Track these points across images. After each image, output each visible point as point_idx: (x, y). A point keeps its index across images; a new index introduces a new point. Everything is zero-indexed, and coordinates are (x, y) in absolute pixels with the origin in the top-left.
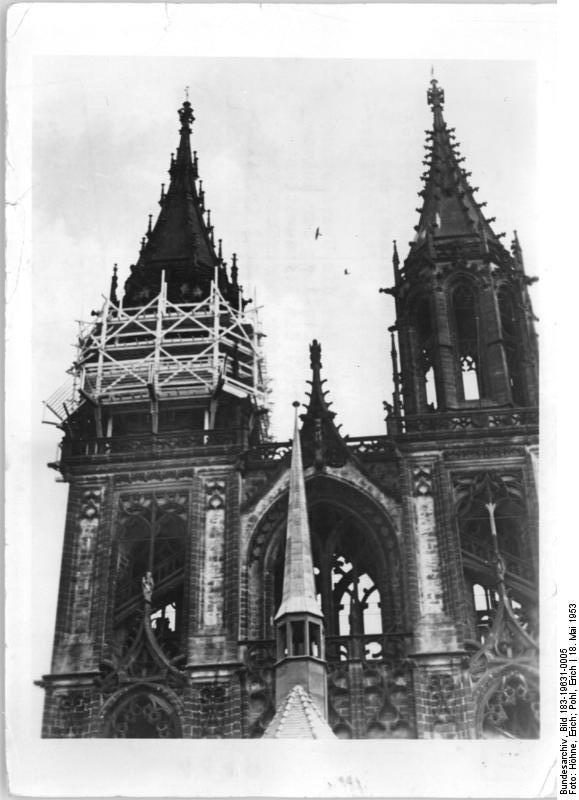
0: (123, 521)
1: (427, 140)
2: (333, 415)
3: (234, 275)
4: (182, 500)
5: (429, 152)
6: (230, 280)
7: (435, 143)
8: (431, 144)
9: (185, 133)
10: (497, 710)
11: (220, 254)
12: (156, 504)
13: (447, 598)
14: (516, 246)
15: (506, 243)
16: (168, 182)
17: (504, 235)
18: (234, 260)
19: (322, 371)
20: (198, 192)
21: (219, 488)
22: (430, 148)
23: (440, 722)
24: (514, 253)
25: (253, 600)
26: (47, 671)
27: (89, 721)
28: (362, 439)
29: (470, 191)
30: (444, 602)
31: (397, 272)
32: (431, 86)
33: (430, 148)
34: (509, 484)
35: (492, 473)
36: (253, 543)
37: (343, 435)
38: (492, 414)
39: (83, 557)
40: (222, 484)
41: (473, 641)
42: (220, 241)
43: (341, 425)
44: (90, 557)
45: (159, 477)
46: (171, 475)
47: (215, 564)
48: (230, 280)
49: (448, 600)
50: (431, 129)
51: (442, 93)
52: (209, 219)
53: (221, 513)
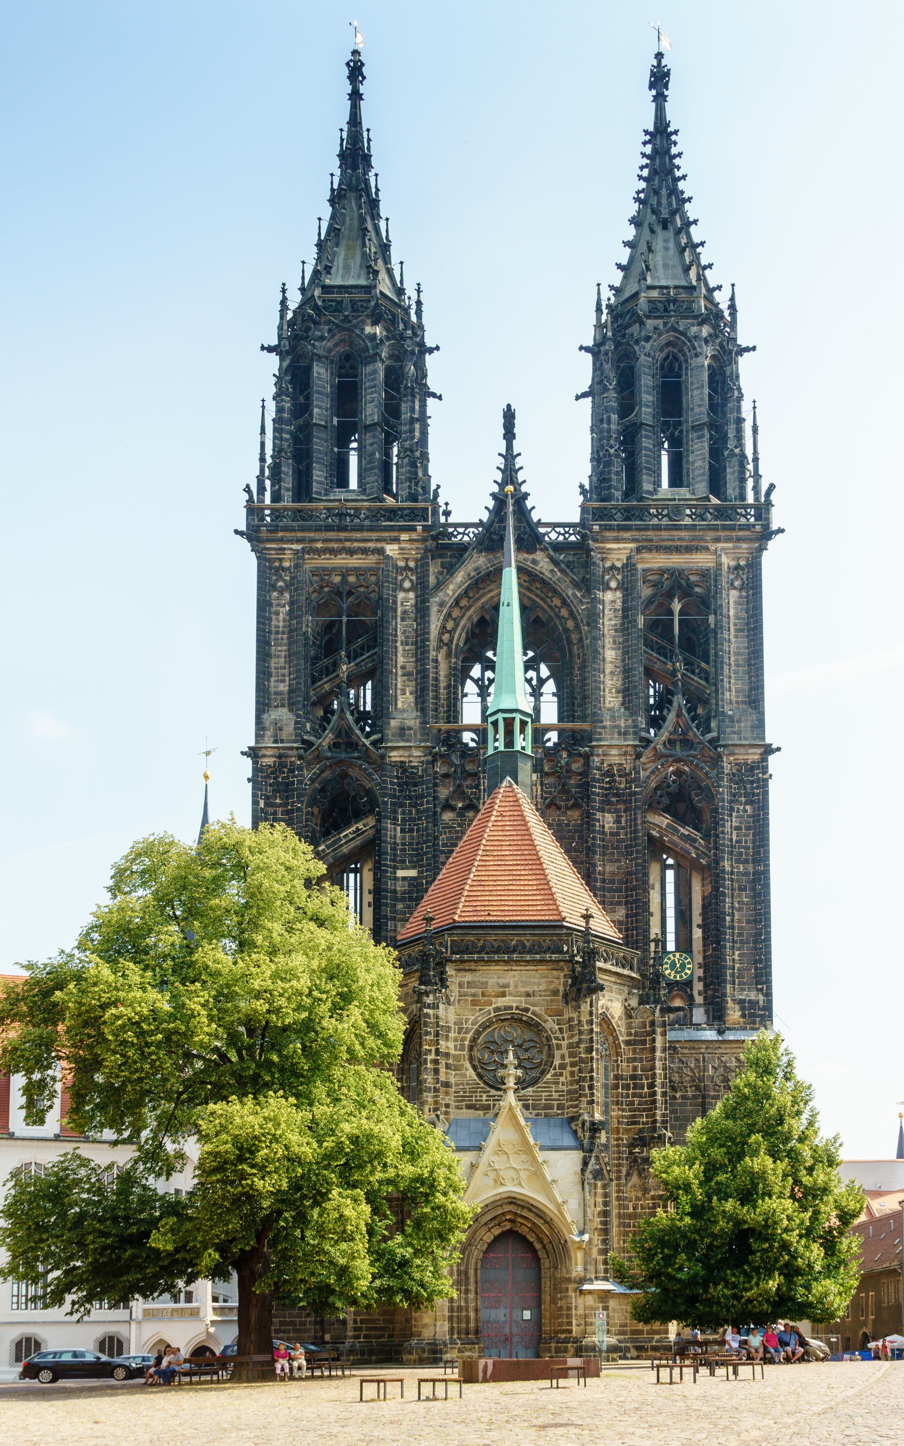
2: (526, 496)
6: (414, 318)
7: (655, 150)
9: (356, 97)
13: (627, 693)
14: (732, 307)
16: (338, 172)
18: (419, 291)
19: (517, 448)
20: (373, 190)
21: (410, 569)
24: (730, 314)
26: (252, 743)
27: (294, 790)
28: (554, 525)
29: (688, 224)
30: (624, 697)
31: (599, 326)
35: (681, 572)
36: (443, 629)
37: (535, 520)
38: (690, 507)
39: (277, 633)
40: (412, 564)
41: (643, 734)
42: (402, 263)
43: (533, 508)
44: (283, 633)
45: (351, 552)
46: (364, 551)
47: (407, 648)
48: (414, 318)
49: (628, 696)
50: (651, 129)
51: (668, 74)
52: (387, 231)
53: (412, 595)
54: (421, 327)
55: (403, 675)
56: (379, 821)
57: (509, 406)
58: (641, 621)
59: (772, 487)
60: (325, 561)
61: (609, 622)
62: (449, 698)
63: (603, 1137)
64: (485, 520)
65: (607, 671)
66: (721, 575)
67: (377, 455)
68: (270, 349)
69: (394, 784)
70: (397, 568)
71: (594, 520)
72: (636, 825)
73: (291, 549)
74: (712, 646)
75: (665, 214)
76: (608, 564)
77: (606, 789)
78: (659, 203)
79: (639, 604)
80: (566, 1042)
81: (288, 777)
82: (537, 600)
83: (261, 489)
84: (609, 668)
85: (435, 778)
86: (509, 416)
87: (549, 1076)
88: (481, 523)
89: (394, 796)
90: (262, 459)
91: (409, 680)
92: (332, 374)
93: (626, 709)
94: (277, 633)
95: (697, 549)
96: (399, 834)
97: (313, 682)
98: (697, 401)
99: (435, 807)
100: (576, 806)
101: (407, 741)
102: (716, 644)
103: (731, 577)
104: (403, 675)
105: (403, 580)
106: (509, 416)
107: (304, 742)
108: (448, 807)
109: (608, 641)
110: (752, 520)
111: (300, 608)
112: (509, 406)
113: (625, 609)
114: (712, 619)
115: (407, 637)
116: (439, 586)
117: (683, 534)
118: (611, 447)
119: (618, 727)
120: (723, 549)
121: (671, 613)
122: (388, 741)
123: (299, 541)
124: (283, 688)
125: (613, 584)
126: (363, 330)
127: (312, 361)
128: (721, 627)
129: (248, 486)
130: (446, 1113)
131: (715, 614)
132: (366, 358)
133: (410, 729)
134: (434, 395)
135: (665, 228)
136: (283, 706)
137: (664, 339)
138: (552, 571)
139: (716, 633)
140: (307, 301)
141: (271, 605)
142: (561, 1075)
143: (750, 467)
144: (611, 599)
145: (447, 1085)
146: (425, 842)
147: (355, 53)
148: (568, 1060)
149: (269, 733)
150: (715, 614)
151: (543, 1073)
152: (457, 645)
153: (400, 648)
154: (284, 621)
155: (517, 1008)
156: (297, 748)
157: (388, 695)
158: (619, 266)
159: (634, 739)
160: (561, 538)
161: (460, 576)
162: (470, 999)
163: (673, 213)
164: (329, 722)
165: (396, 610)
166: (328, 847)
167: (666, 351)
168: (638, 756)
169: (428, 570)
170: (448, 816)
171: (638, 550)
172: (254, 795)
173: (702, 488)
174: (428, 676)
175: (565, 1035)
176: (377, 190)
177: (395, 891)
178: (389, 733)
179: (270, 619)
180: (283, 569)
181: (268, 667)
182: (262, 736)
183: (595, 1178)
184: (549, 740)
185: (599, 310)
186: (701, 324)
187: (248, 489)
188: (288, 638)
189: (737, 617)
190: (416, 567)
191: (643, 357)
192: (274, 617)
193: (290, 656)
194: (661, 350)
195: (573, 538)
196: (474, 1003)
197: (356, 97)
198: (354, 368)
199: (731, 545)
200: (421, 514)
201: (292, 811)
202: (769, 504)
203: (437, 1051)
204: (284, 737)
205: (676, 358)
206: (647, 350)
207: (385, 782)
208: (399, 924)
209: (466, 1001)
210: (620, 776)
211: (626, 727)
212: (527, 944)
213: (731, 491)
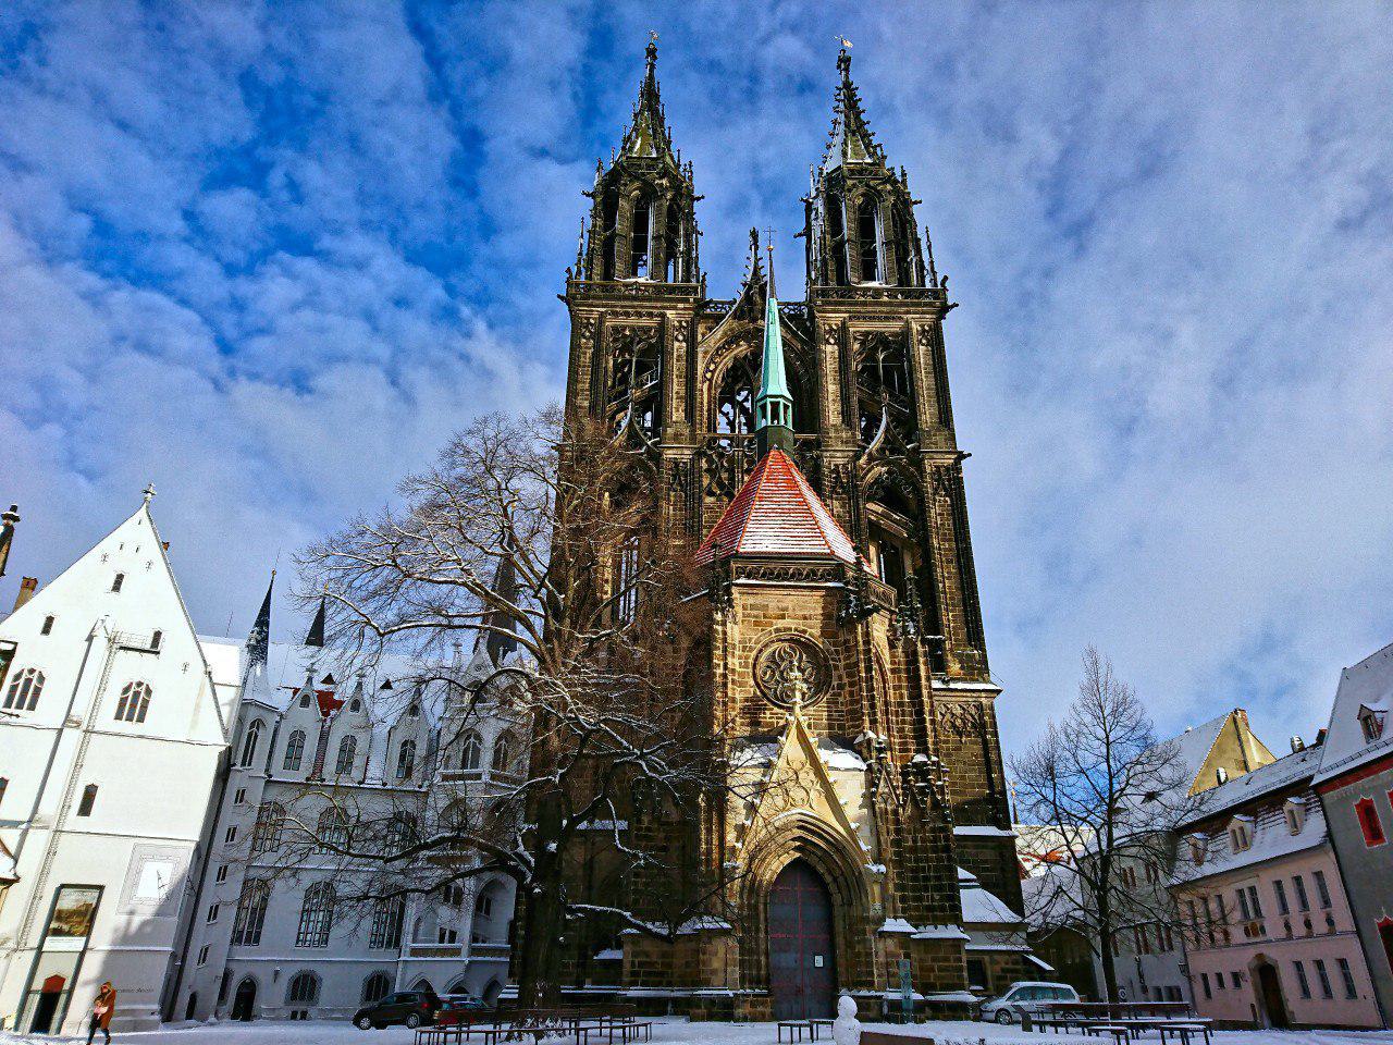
13: (846, 414)
36: (707, 370)
39: (584, 366)
40: (684, 324)
51: (849, 59)
59: (946, 278)
68: (588, 195)
80: (843, 663)
96: (671, 512)
117: (882, 309)
121: (877, 361)
124: (586, 404)
142: (840, 695)
148: (846, 680)
153: (675, 380)
155: (796, 630)
175: (842, 657)
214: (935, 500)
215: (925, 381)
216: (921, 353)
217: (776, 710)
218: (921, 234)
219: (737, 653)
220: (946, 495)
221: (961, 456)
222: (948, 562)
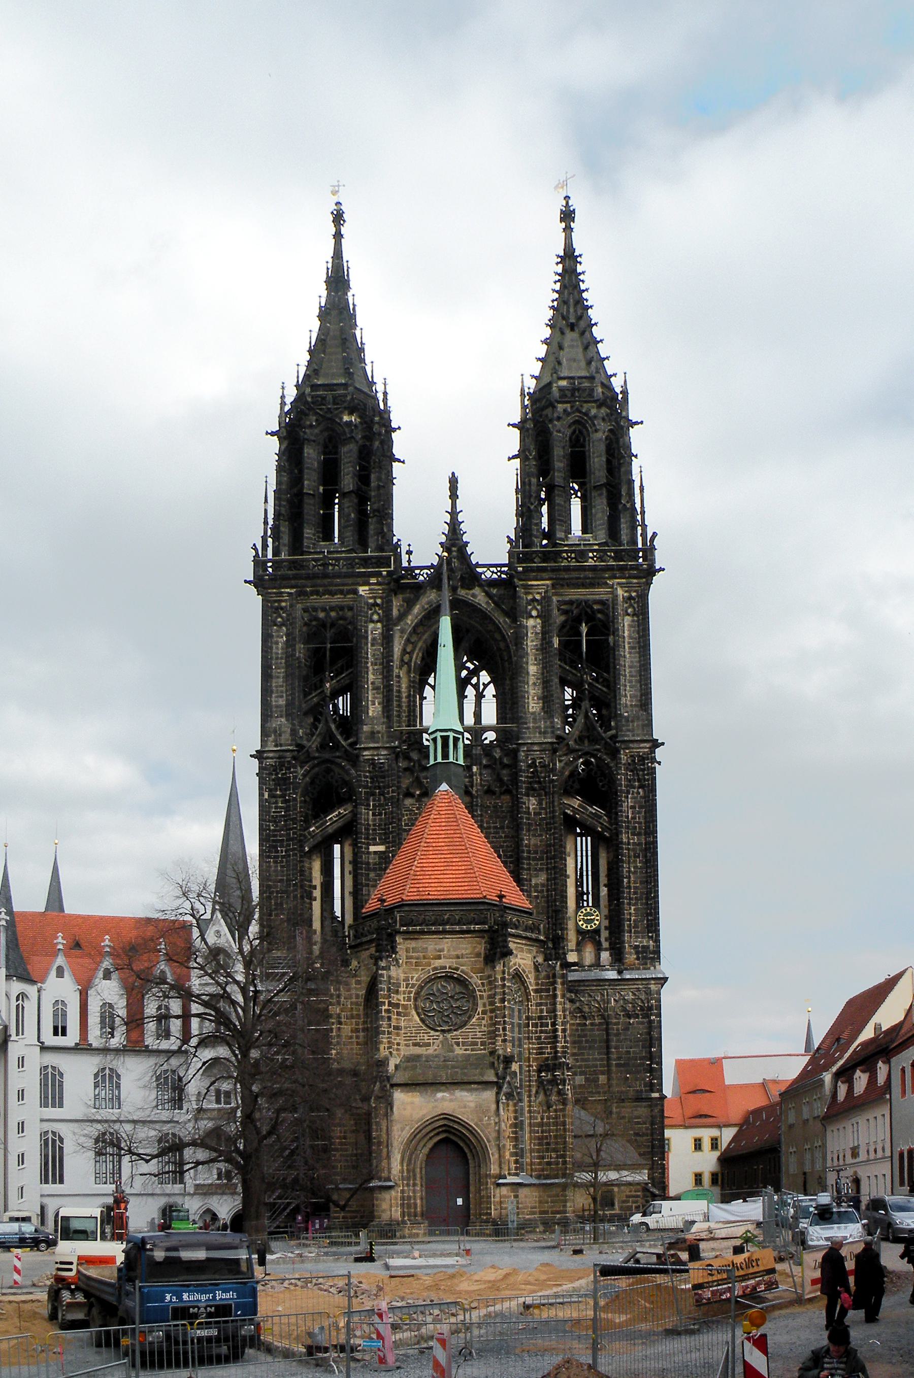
0: (305, 629)
1: (557, 263)
3: (385, 404)
4: (349, 614)
5: (558, 278)
6: (382, 407)
8: (559, 269)
9: (338, 236)
10: (574, 782)
11: (372, 377)
12: (330, 617)
13: (547, 699)
14: (625, 392)
15: (617, 384)
16: (324, 293)
17: (615, 375)
18: (385, 384)
20: (351, 307)
21: (378, 605)
22: (559, 274)
23: (534, 789)
25: (404, 695)
26: (259, 748)
30: (543, 703)
31: (524, 407)
32: (564, 203)
33: (559, 274)
34: (599, 611)
36: (404, 652)
37: (474, 563)
38: (593, 551)
39: (277, 658)
40: (379, 601)
44: (281, 658)
45: (332, 594)
46: (341, 592)
47: (376, 667)
50: (562, 254)
53: (379, 625)
54: (387, 411)
55: (373, 689)
56: (355, 807)
57: (453, 474)
58: (556, 642)
59: (655, 535)
60: (314, 600)
61: (531, 643)
62: (409, 706)
63: (515, 1067)
64: (435, 564)
65: (531, 683)
66: (617, 604)
67: (353, 515)
68: (273, 434)
69: (367, 777)
70: (367, 603)
71: (518, 563)
72: (553, 806)
73: (285, 593)
74: (611, 660)
75: (572, 320)
76: (530, 597)
77: (531, 777)
78: (568, 311)
79: (555, 629)
81: (286, 773)
82: (476, 625)
83: (265, 546)
84: (532, 679)
85: (399, 771)
86: (453, 482)
87: (474, 1020)
88: (432, 566)
89: (366, 787)
90: (266, 523)
91: (378, 693)
92: (318, 453)
93: (545, 712)
94: (277, 658)
95: (599, 585)
96: (371, 817)
97: (305, 696)
98: (597, 466)
99: (398, 794)
100: (508, 792)
101: (378, 742)
102: (614, 659)
103: (626, 605)
104: (373, 689)
105: (372, 614)
106: (453, 482)
107: (298, 745)
108: (409, 795)
109: (531, 659)
110: (641, 560)
111: (294, 639)
112: (453, 474)
113: (544, 633)
114: (611, 639)
115: (376, 659)
116: (402, 616)
118: (532, 504)
119: (539, 727)
120: (618, 584)
121: (580, 635)
122: (361, 743)
123: (291, 587)
124: (282, 702)
125: (534, 613)
126: (341, 419)
127: (303, 444)
128: (619, 645)
129: (254, 545)
130: (398, 1050)
131: (614, 634)
132: (345, 440)
133: (378, 732)
134: (399, 461)
135: (572, 329)
136: (281, 717)
137: (570, 419)
138: (487, 603)
139: (614, 650)
140: (299, 398)
141: (272, 636)
142: (483, 1019)
143: (639, 517)
144: (532, 624)
145: (397, 1028)
146: (391, 824)
147: (338, 203)
149: (271, 739)
150: (614, 634)
151: (470, 1017)
152: (415, 663)
153: (371, 668)
154: (282, 648)
156: (292, 751)
157: (362, 706)
158: (539, 359)
159: (552, 738)
160: (495, 576)
161: (416, 609)
162: (414, 961)
163: (580, 318)
164: (316, 729)
165: (367, 638)
166: (317, 828)
167: (573, 428)
168: (555, 751)
169: (392, 606)
170: (408, 802)
171: (553, 586)
172: (260, 789)
173: (602, 535)
174: (392, 690)
176: (354, 305)
177: (368, 863)
178: (363, 737)
179: (271, 648)
180: (282, 608)
181: (271, 686)
182: (266, 741)
183: (507, 1099)
184: (486, 739)
185: (522, 394)
186: (599, 407)
187: (255, 547)
188: (285, 663)
189: (630, 637)
190: (383, 603)
191: (555, 433)
192: (274, 646)
193: (287, 676)
194: (570, 426)
195: (503, 576)
196: (417, 964)
197: (338, 236)
198: (336, 447)
199: (624, 581)
200: (385, 562)
201: (289, 801)
202: (653, 548)
203: (389, 1002)
204: (282, 742)
205: (580, 432)
206: (557, 428)
207: (360, 776)
208: (372, 889)
209: (411, 963)
210: (541, 767)
211: (546, 727)
212: (457, 917)
213: (624, 538)
214: (628, 792)
215: (627, 657)
216: (626, 625)
217: (432, 1033)
218: (636, 477)
219: (402, 989)
220: (639, 787)
221: (656, 744)
222: (635, 857)
